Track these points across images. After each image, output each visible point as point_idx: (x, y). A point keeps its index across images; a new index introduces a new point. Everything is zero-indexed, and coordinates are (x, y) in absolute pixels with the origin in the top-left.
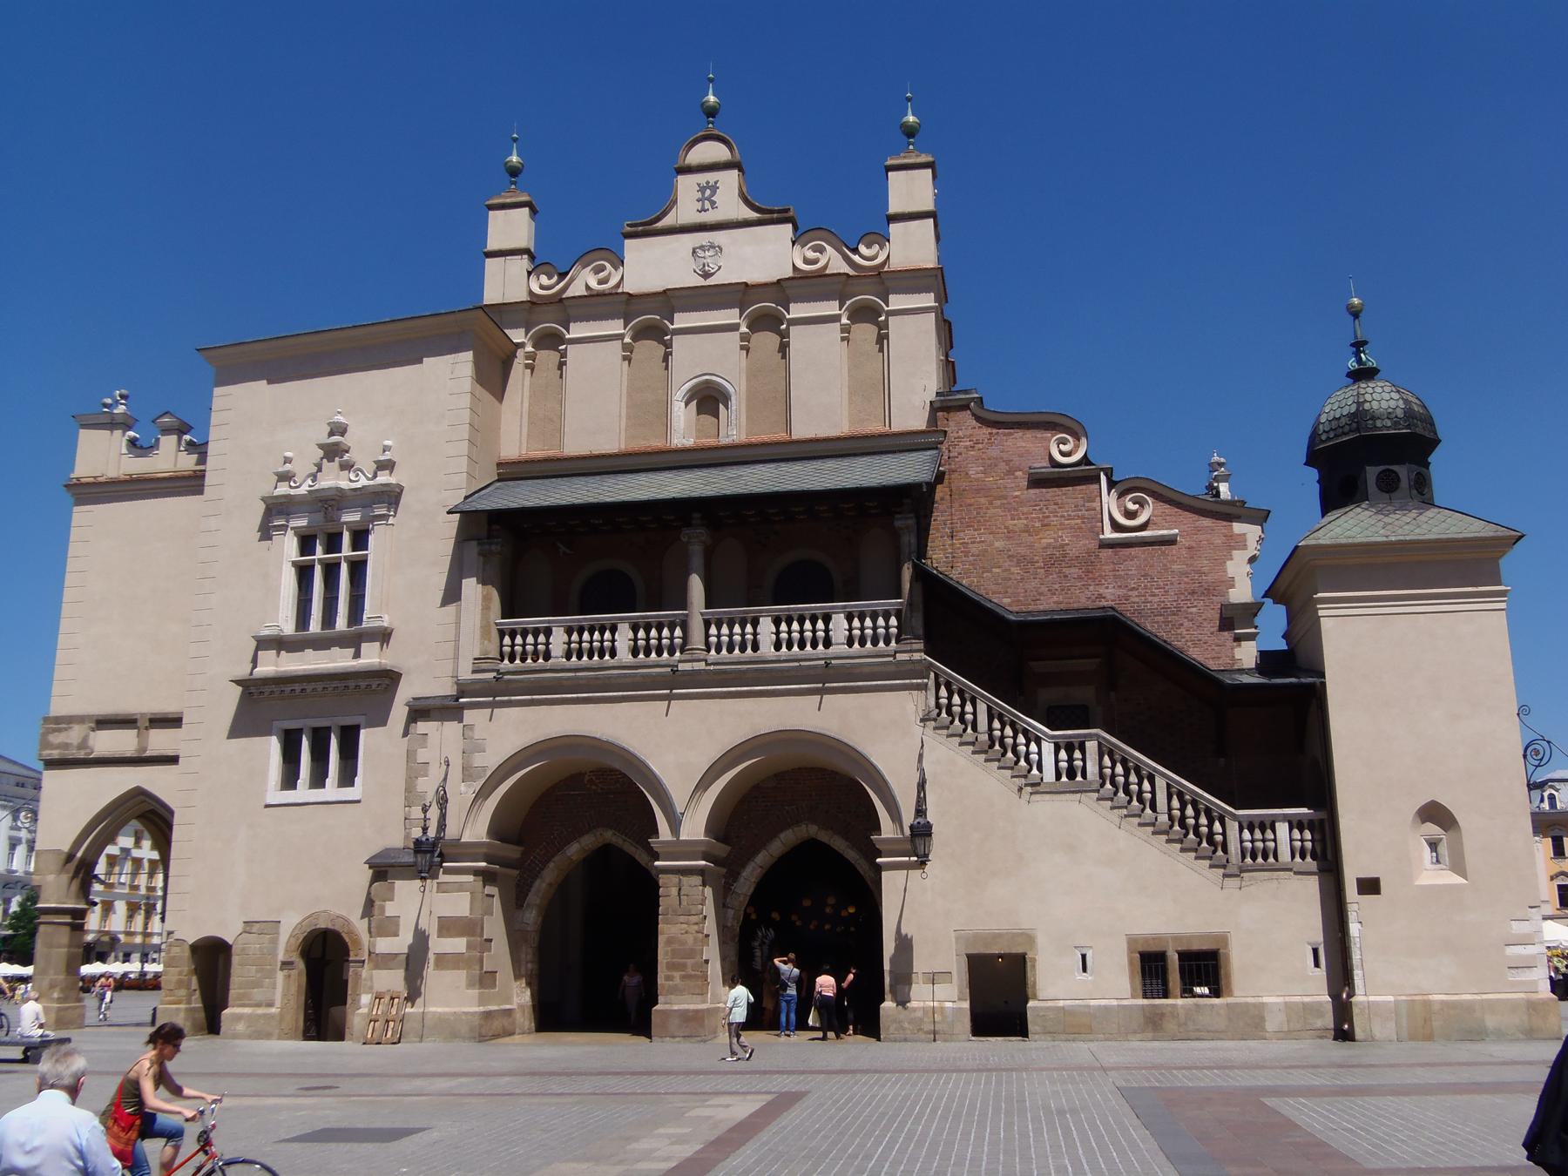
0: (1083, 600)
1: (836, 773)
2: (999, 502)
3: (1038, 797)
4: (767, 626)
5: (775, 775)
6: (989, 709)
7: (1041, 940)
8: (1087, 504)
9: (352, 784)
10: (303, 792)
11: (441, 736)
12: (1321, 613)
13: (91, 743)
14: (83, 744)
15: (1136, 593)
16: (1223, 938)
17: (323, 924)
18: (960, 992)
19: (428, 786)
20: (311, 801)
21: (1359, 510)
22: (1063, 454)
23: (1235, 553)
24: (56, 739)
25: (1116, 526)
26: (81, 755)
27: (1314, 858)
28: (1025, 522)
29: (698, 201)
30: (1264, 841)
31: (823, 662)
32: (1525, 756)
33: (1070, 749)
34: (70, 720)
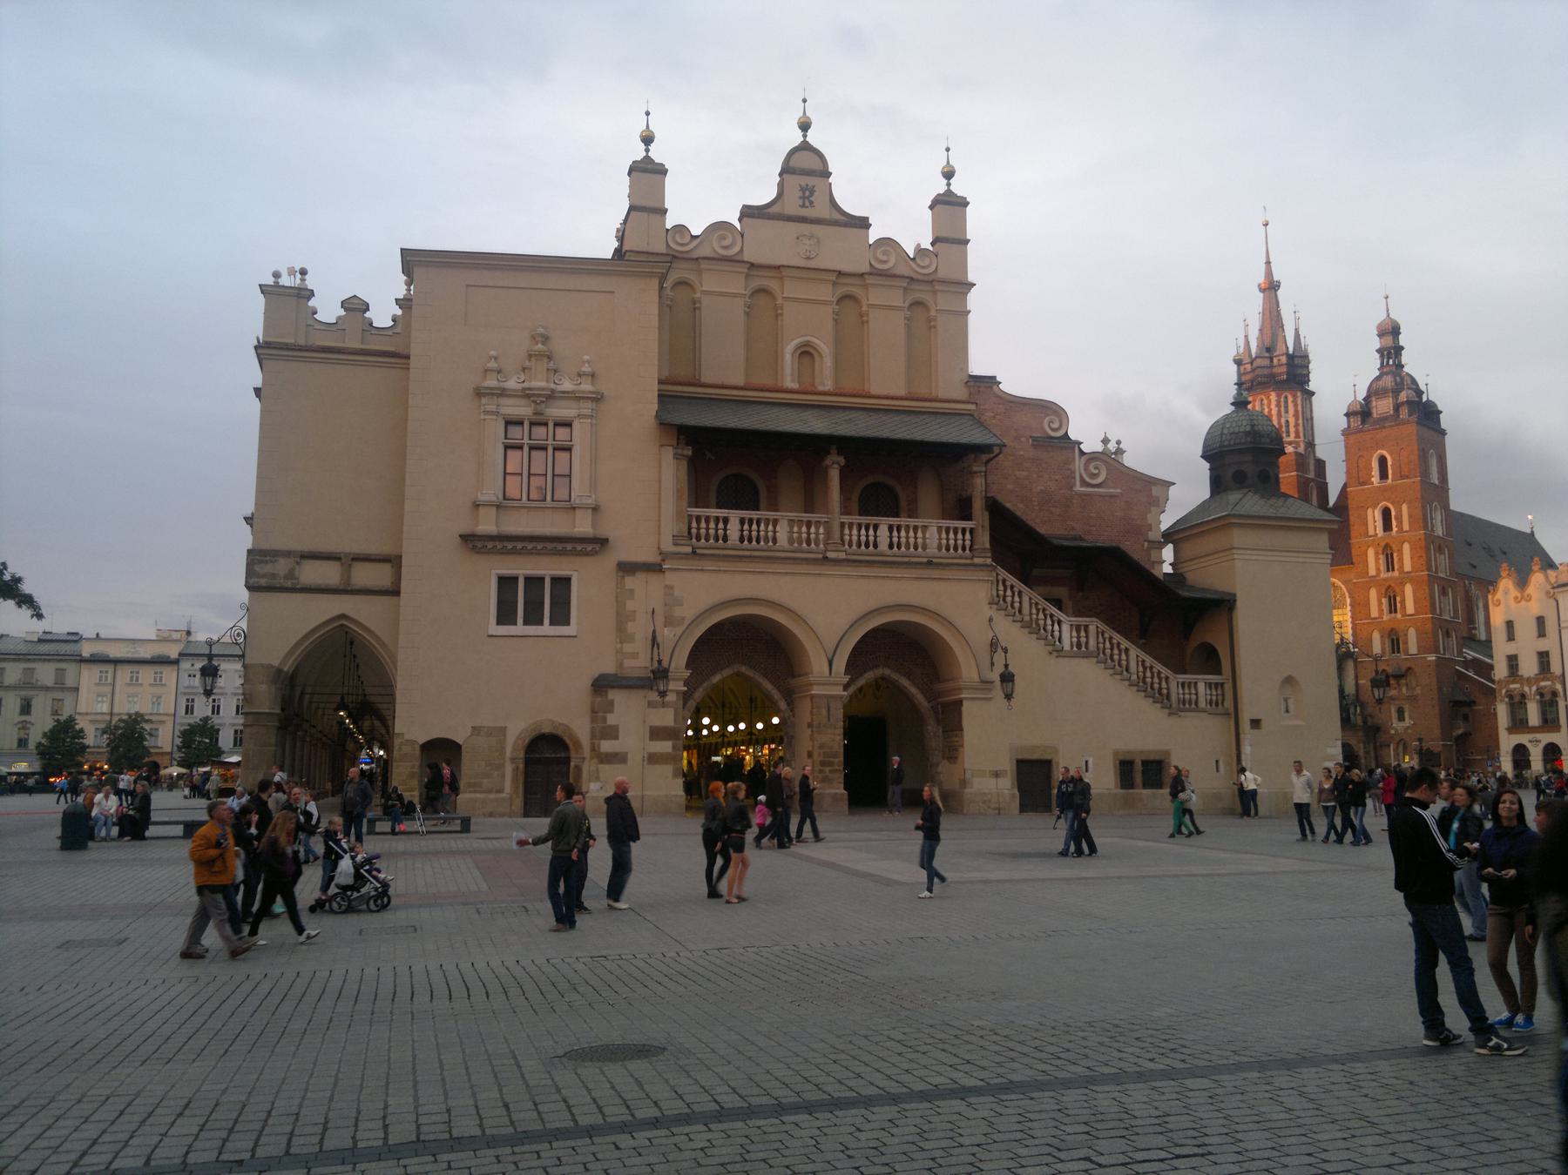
3: (1061, 660)
4: (883, 531)
6: (1030, 599)
9: (568, 624)
11: (646, 591)
13: (297, 573)
14: (291, 575)
16: (1167, 753)
17: (546, 729)
18: (1013, 784)
19: (640, 629)
22: (1052, 430)
23: (1153, 509)
25: (1084, 483)
26: (289, 584)
29: (801, 198)
30: (1190, 694)
33: (1078, 629)
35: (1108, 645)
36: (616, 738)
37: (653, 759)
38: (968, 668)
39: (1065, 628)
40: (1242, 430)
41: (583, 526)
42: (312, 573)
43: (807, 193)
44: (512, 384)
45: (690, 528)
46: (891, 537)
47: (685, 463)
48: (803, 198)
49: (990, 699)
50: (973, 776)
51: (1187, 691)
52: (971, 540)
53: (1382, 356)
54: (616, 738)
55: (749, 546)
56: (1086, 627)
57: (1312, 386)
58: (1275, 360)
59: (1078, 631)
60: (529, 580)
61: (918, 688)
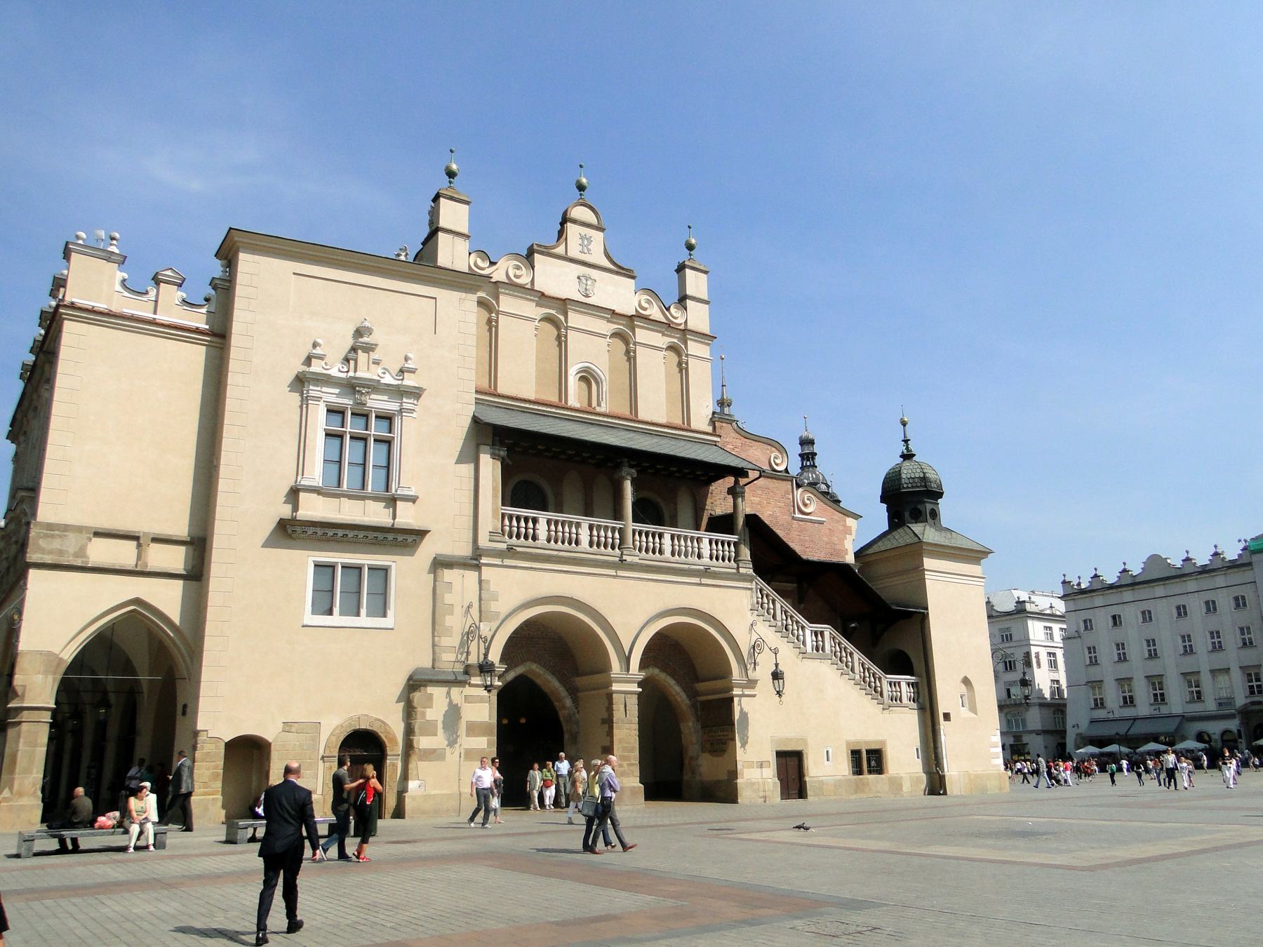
1: (668, 637)
4: (667, 540)
6: (782, 606)
7: (809, 741)
11: (462, 583)
12: (926, 577)
16: (884, 742)
17: (364, 726)
19: (455, 623)
20: (309, 624)
22: (777, 465)
26: (79, 563)
27: (914, 701)
30: (896, 692)
31: (702, 568)
39: (808, 632)
41: (407, 516)
43: (586, 242)
44: (334, 372)
45: (503, 525)
49: (754, 696)
50: (744, 767)
53: (803, 459)
55: (556, 547)
56: (822, 633)
59: (816, 636)
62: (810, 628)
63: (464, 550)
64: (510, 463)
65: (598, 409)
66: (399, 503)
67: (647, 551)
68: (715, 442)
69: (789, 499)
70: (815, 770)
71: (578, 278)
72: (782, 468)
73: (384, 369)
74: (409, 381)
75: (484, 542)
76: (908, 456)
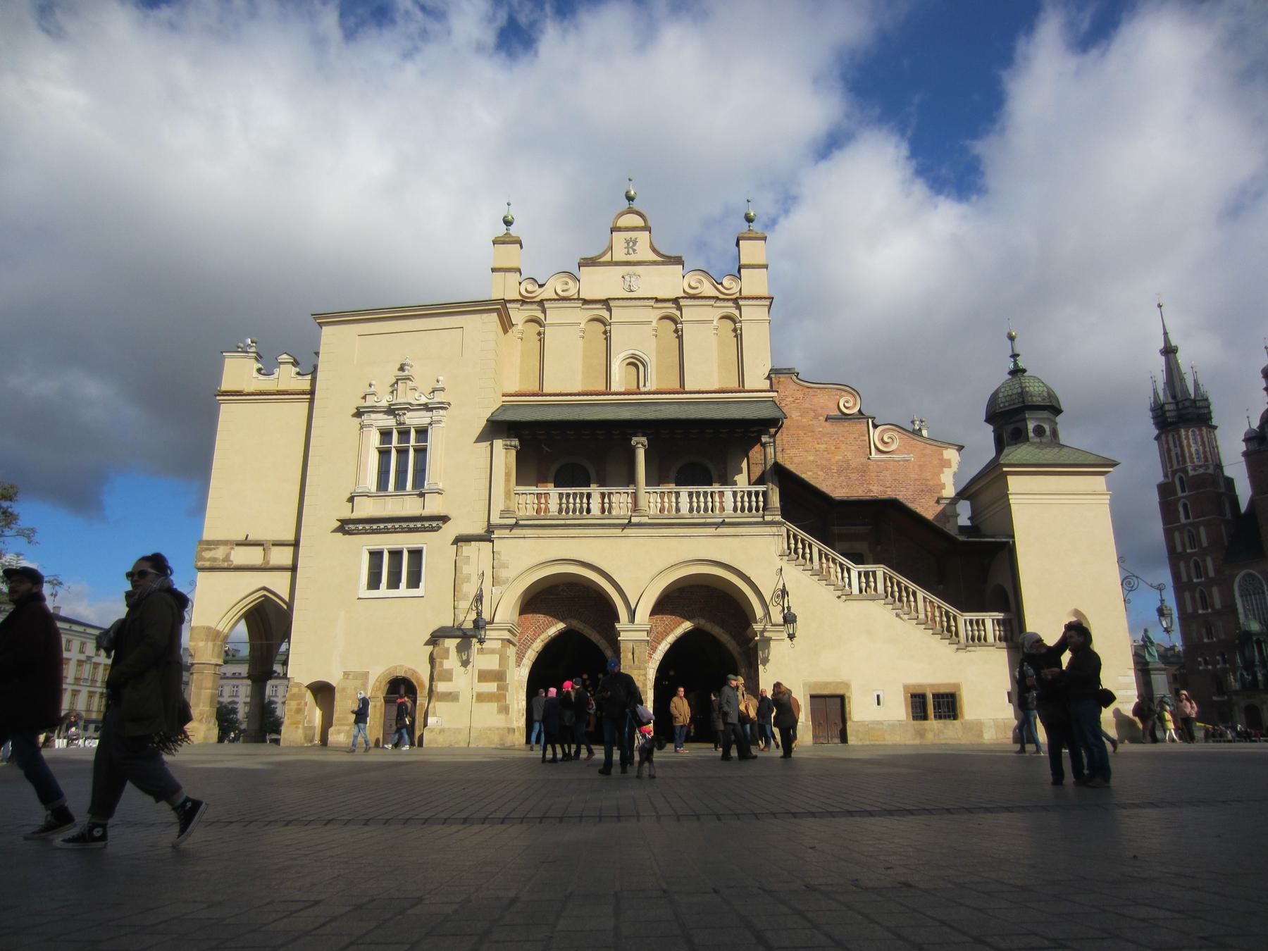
0: (860, 492)
1: (716, 589)
2: (810, 434)
4: (684, 498)
5: (679, 589)
6: (820, 550)
8: (862, 438)
10: (383, 590)
13: (232, 558)
15: (889, 489)
16: (958, 686)
17: (400, 673)
19: (470, 590)
21: (1025, 446)
22: (847, 408)
23: (945, 469)
24: (207, 555)
26: (226, 565)
28: (825, 446)
32: (1122, 584)
34: (217, 543)
35: (896, 588)
36: (450, 679)
37: (481, 698)
38: (766, 618)
39: (854, 574)
40: (1015, 391)
41: (433, 506)
42: (241, 556)
43: (631, 244)
46: (691, 503)
47: (514, 452)
48: (628, 248)
51: (975, 628)
52: (764, 502)
54: (450, 679)
55: (567, 517)
56: (874, 573)
57: (1214, 422)
58: (1180, 406)
60: (392, 553)
61: (731, 634)
62: (855, 570)
63: (479, 529)
64: (549, 450)
65: (643, 389)
66: (426, 495)
67: (698, 511)
68: (772, 397)
69: (865, 440)
70: (860, 712)
71: (623, 277)
72: (855, 410)
73: (421, 393)
74: (439, 397)
75: (493, 521)
76: (1017, 372)
